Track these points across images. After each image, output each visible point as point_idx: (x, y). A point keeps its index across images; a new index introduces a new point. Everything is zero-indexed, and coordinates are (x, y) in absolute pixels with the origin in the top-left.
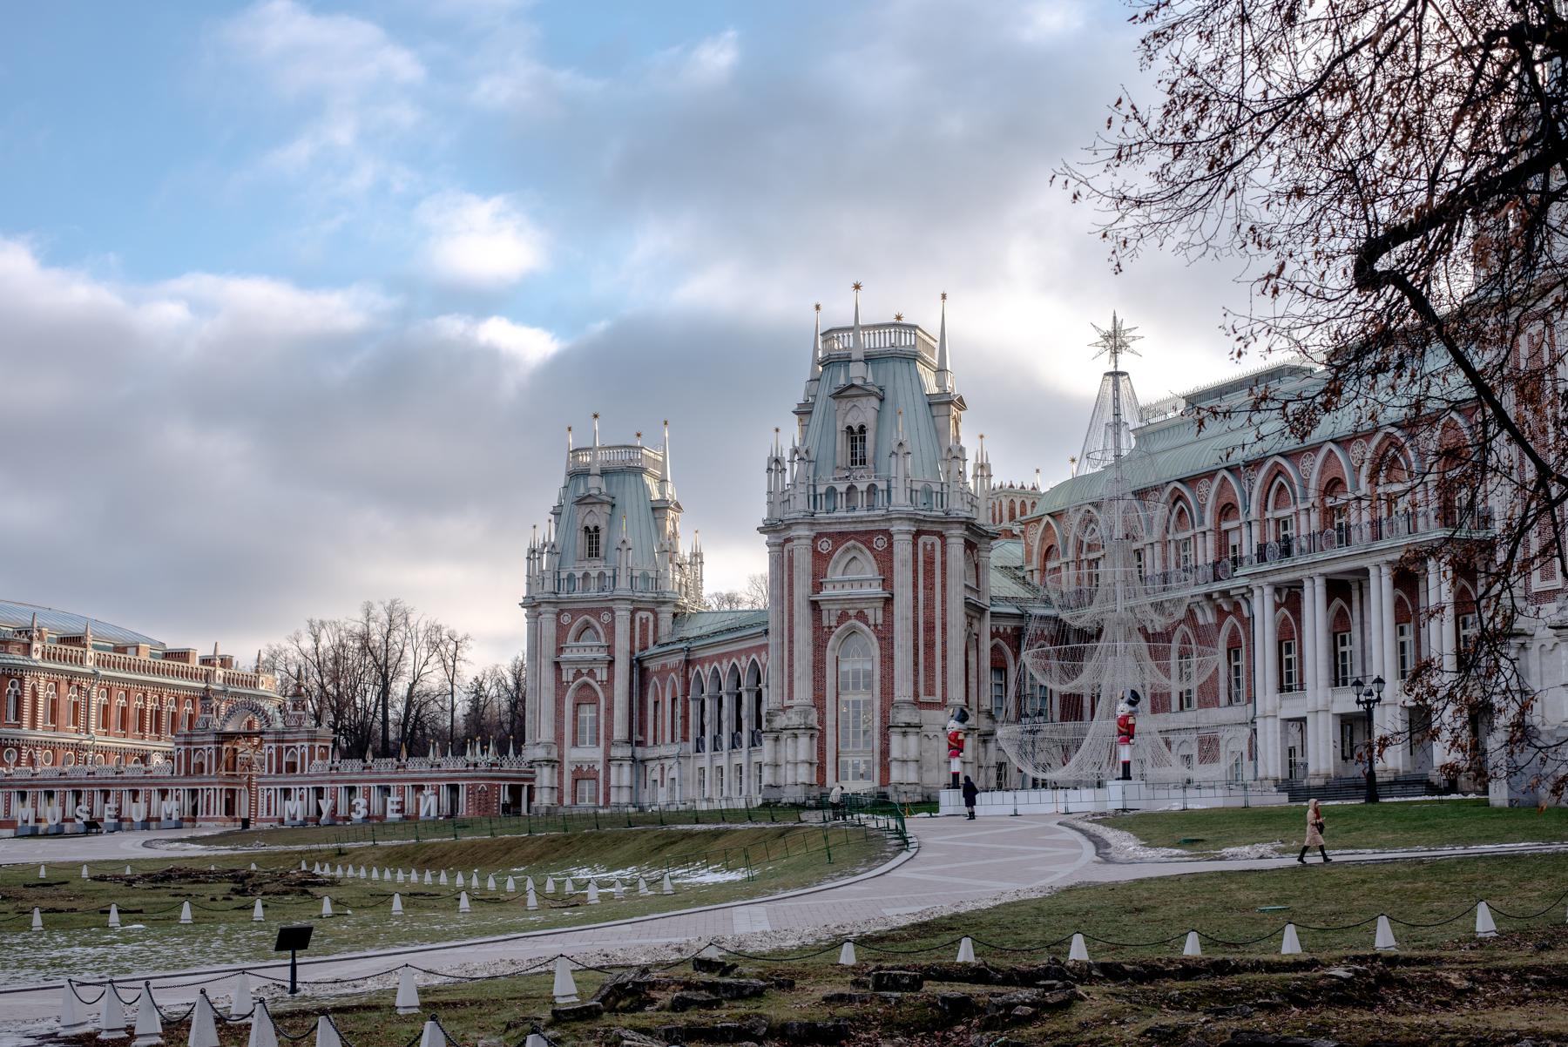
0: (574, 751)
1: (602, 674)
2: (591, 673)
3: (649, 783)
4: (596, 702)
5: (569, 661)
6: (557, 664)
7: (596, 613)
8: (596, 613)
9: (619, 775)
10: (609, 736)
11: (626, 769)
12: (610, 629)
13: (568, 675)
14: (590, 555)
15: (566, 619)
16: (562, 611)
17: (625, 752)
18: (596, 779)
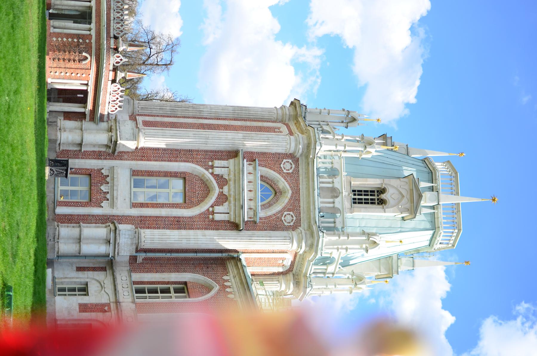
0: (127, 173)
1: (221, 213)
2: (222, 199)
3: (84, 277)
4: (187, 203)
5: (239, 173)
6: (233, 154)
7: (294, 205)
8: (294, 205)
9: (94, 240)
10: (144, 222)
11: (102, 249)
12: (273, 225)
13: (221, 167)
14: (354, 191)
15: (287, 166)
16: (296, 161)
17: (126, 249)
18: (90, 203)
